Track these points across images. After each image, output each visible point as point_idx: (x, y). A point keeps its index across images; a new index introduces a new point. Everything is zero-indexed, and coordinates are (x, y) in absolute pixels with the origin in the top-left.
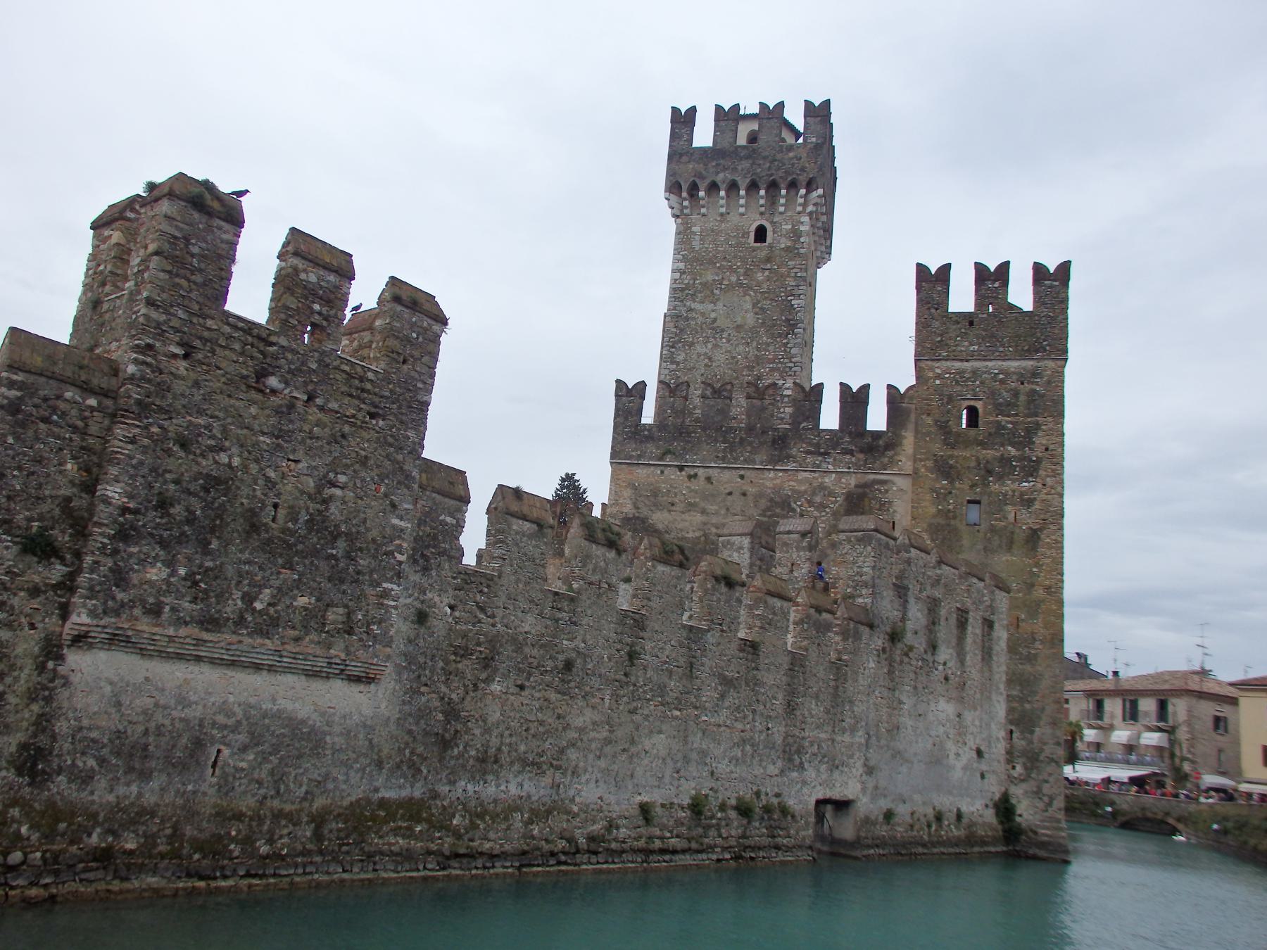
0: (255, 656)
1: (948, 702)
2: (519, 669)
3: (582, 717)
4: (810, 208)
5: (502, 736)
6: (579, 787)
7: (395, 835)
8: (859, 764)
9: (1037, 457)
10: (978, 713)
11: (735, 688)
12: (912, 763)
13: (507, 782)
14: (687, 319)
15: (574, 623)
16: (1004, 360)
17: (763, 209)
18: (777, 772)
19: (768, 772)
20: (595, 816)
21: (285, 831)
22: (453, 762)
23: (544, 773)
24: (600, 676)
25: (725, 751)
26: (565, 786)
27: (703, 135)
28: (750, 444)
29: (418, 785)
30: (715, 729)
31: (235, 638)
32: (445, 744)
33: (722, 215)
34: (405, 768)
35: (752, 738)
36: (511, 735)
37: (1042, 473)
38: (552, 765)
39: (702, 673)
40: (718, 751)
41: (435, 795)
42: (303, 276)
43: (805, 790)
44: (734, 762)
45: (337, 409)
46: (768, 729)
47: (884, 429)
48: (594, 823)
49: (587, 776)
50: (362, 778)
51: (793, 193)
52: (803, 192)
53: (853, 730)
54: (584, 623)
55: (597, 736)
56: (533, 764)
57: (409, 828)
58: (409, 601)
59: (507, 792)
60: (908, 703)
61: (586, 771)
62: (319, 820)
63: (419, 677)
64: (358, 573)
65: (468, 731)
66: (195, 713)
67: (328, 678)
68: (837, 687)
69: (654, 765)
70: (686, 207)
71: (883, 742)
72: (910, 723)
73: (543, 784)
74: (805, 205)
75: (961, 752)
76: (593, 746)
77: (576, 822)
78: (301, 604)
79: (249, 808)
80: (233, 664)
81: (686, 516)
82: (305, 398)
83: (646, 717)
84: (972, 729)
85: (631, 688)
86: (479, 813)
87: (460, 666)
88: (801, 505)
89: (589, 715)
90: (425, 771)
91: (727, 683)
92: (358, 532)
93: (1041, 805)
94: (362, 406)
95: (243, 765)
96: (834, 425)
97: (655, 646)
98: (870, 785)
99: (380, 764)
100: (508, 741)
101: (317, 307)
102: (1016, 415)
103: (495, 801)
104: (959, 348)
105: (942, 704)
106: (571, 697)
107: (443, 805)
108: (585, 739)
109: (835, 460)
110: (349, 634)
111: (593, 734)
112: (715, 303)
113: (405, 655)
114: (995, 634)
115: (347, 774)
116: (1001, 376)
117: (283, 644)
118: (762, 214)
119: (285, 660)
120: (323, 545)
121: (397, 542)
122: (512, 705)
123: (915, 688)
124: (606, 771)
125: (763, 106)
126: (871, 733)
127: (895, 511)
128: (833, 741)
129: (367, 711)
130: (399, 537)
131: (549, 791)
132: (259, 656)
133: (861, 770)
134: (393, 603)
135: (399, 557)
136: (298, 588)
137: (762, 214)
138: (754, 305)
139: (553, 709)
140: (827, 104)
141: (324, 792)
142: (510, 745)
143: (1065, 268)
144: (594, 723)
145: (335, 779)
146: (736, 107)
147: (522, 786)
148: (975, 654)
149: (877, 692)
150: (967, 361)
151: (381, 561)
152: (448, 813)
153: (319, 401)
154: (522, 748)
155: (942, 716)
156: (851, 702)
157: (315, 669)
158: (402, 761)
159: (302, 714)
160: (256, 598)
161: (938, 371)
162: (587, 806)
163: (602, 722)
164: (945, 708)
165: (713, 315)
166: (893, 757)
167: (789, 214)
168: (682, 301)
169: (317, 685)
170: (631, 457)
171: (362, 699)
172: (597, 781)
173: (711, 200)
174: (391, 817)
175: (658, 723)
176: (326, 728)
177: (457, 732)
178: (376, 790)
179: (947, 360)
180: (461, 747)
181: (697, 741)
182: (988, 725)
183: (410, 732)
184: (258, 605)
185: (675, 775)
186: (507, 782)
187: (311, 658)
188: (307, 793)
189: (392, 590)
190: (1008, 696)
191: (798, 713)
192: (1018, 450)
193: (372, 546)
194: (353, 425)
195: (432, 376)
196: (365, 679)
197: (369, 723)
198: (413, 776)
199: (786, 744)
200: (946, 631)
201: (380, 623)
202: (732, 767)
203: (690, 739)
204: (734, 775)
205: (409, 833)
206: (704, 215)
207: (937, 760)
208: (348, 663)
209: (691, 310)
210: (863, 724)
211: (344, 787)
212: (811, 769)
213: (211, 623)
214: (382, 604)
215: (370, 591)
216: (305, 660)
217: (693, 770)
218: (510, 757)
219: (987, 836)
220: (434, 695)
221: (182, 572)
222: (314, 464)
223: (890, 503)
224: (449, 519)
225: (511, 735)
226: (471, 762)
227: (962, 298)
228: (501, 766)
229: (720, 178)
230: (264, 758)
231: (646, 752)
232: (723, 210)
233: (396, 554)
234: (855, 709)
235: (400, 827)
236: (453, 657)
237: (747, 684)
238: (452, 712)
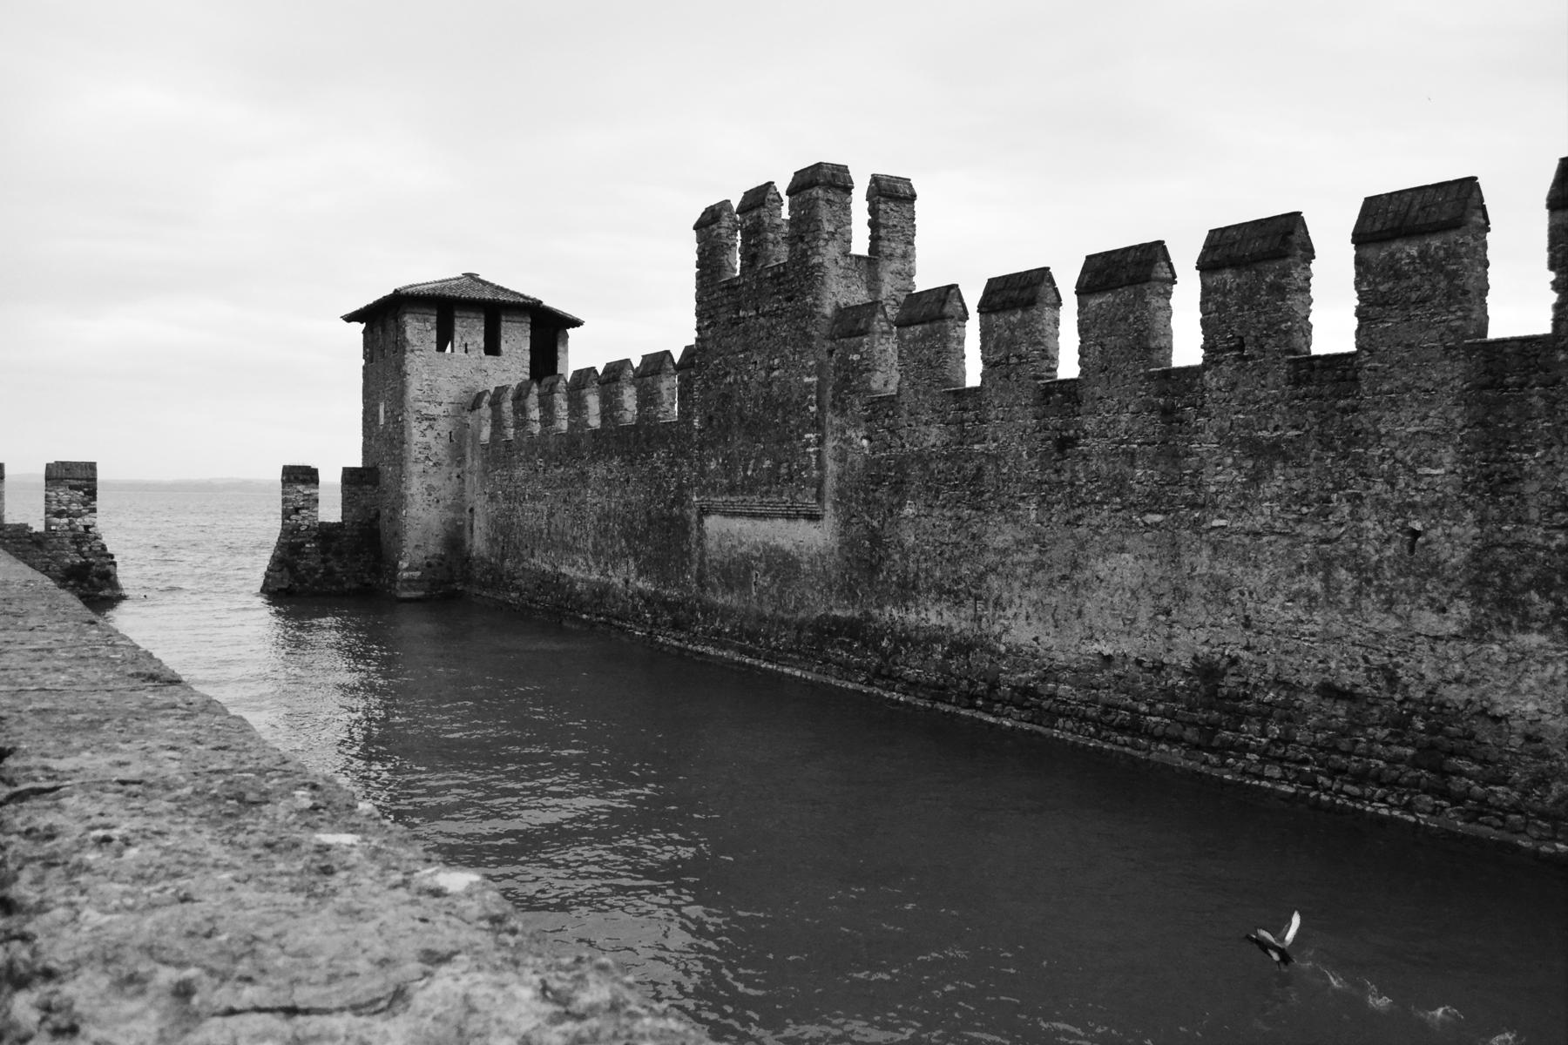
3: (1002, 535)
6: (1006, 623)
7: (841, 648)
23: (962, 602)
25: (1274, 581)
29: (857, 606)
30: (1247, 541)
32: (874, 569)
36: (926, 560)
38: (970, 594)
41: (869, 618)
44: (1304, 601)
49: (1014, 610)
55: (1023, 558)
56: (949, 592)
57: (850, 644)
59: (927, 621)
61: (1011, 602)
62: (800, 627)
65: (889, 556)
69: (1116, 599)
73: (962, 615)
76: (1020, 571)
85: (1068, 490)
86: (906, 639)
87: (877, 494)
100: (924, 566)
103: (917, 628)
106: (986, 512)
108: (1008, 561)
111: (1018, 557)
142: (926, 570)
144: (1018, 542)
154: (938, 574)
159: (787, 548)
169: (792, 524)
172: (1027, 617)
174: (839, 633)
175: (1117, 537)
177: (880, 558)
183: (848, 559)
184: (749, 473)
185: (1162, 618)
191: (1531, 488)
196: (813, 517)
203: (1186, 559)
204: (1304, 628)
205: (850, 650)
217: (1197, 610)
225: (926, 560)
228: (919, 593)
238: (875, 537)
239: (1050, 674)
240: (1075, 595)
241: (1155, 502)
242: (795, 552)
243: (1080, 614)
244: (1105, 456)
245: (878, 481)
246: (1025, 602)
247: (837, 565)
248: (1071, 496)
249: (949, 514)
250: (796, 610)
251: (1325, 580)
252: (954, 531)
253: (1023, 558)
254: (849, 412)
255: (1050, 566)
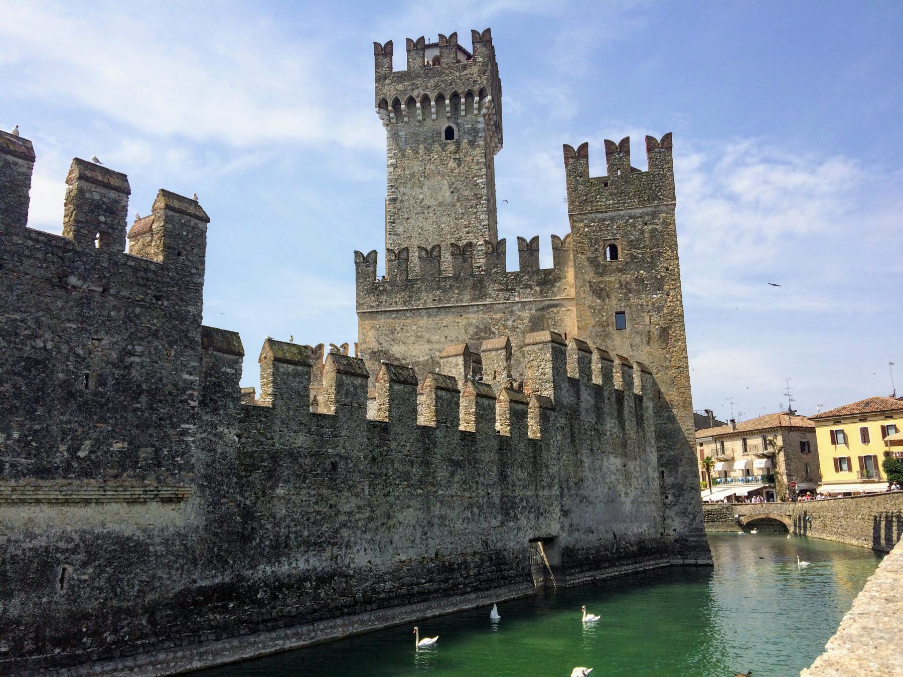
0: (84, 493)
1: (616, 457)
2: (297, 475)
3: (348, 503)
4: (484, 111)
5: (289, 527)
8: (558, 509)
9: (661, 276)
10: (638, 462)
11: (461, 467)
12: (595, 504)
13: (297, 560)
14: (402, 201)
15: (336, 436)
16: (631, 209)
17: (449, 115)
18: (498, 524)
19: (492, 525)
20: (367, 576)
21: (126, 622)
22: (252, 552)
24: (359, 472)
25: (458, 515)
26: (341, 557)
27: (400, 62)
28: (458, 288)
29: (228, 573)
31: (64, 481)
32: (245, 539)
33: (420, 121)
34: (215, 562)
35: (477, 502)
36: (296, 525)
37: (666, 287)
38: (329, 543)
39: (437, 460)
40: (453, 515)
41: (242, 578)
42: (88, 195)
43: (520, 534)
45: (128, 296)
46: (489, 494)
47: (552, 267)
48: (367, 581)
50: (181, 575)
51: (470, 100)
52: (477, 99)
53: (550, 486)
54: (343, 434)
55: (362, 516)
56: (315, 544)
57: (225, 607)
58: (204, 435)
60: (587, 461)
62: (151, 610)
63: (219, 491)
64: (161, 419)
65: (262, 527)
66: (41, 542)
67: (145, 502)
68: (536, 457)
70: (393, 118)
71: (573, 492)
72: (590, 475)
73: (324, 558)
74: (479, 109)
75: (629, 491)
76: (360, 524)
77: (353, 582)
78: (116, 449)
79: (94, 609)
80: (66, 502)
81: (416, 346)
82: (101, 289)
83: (398, 498)
84: (634, 474)
85: (384, 478)
88: (499, 329)
89: (354, 502)
90: (231, 562)
91: (456, 464)
92: (157, 388)
93: (688, 521)
94: (149, 291)
95: (85, 577)
96: (517, 269)
97: (399, 445)
98: (567, 524)
99: (195, 562)
100: (294, 530)
101: (102, 219)
102: (644, 247)
104: (599, 203)
105: (612, 459)
107: (248, 585)
108: (353, 520)
109: (519, 293)
110: (158, 467)
111: (357, 516)
112: (421, 187)
113: (205, 476)
114: (644, 405)
115: (169, 573)
116: (631, 221)
117: (105, 481)
118: (448, 118)
119: (109, 493)
120: (128, 402)
121: (189, 392)
122: (294, 502)
123: (592, 450)
124: (369, 542)
125: (441, 36)
126: (564, 486)
127: (565, 326)
128: (537, 496)
129: (180, 523)
130: (191, 388)
131: (329, 562)
132: (87, 493)
133: (559, 514)
134: (191, 439)
135: (192, 403)
136: (113, 437)
137: (448, 118)
138: (450, 187)
139: (326, 501)
140: (488, 31)
141: (153, 589)
143: (668, 137)
144: (358, 507)
145: (161, 578)
146: (422, 39)
147: (308, 561)
148: (632, 421)
149: (564, 457)
150: (606, 212)
151: (178, 408)
152: (253, 589)
153: (112, 291)
154: (306, 533)
155: (613, 468)
156: (547, 467)
157: (134, 497)
158: (212, 557)
159: (127, 533)
160: (78, 449)
161: (586, 221)
162: (360, 569)
163: (365, 506)
164: (614, 462)
165: (421, 197)
166: (581, 501)
167: (469, 116)
168: (397, 188)
169: (138, 509)
170: (372, 307)
171: (174, 514)
172: (365, 550)
173: (411, 111)
174: (208, 599)
176: (148, 541)
177: (253, 528)
178: (195, 581)
179: (591, 213)
180: (258, 540)
181: (437, 510)
182: (646, 470)
183: (216, 534)
184: (81, 454)
185: (424, 537)
186: (297, 560)
187: (130, 489)
188: (139, 591)
189: (189, 429)
190: (658, 447)
191: (509, 480)
192: (648, 272)
193: (169, 398)
194: (142, 307)
195: (203, 263)
197: (182, 532)
198: (223, 567)
199: (502, 503)
200: (609, 407)
201: (182, 455)
202: (465, 525)
203: (432, 509)
204: (467, 531)
205: (225, 610)
206: (406, 123)
207: (612, 500)
208: (160, 488)
209: (404, 194)
210: (557, 481)
211: (169, 583)
212: (523, 518)
213: (43, 472)
214: (183, 441)
215: (171, 432)
216: (125, 491)
217: (436, 530)
218: (297, 542)
219: (653, 547)
220: (232, 504)
221: (16, 435)
222: (114, 340)
223: (562, 320)
224: (228, 370)
225: (296, 525)
226: (267, 549)
227: (598, 168)
228: (291, 549)
229: (415, 94)
230: (101, 570)
231: (400, 523)
232: (420, 118)
233: (189, 401)
234: (550, 471)
235: (216, 607)
236: (243, 474)
237: (470, 464)
238: (248, 514)
239: (380, 579)
240: (389, 533)
241: (422, 483)
242: (139, 534)
243: (391, 542)
244: (402, 462)
245: (251, 468)
246: (364, 542)
247: (202, 540)
248: (385, 480)
249: (312, 492)
250: (141, 593)
251: (471, 512)
252: (316, 503)
253: (362, 516)
254: (222, 412)
255: (377, 519)
